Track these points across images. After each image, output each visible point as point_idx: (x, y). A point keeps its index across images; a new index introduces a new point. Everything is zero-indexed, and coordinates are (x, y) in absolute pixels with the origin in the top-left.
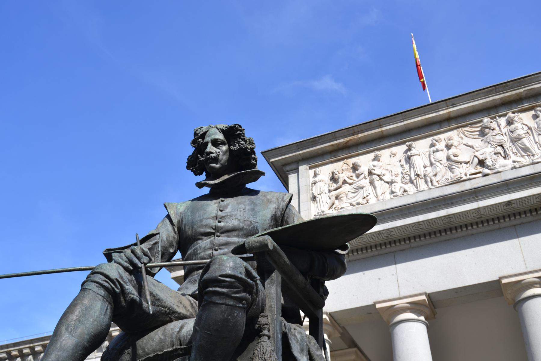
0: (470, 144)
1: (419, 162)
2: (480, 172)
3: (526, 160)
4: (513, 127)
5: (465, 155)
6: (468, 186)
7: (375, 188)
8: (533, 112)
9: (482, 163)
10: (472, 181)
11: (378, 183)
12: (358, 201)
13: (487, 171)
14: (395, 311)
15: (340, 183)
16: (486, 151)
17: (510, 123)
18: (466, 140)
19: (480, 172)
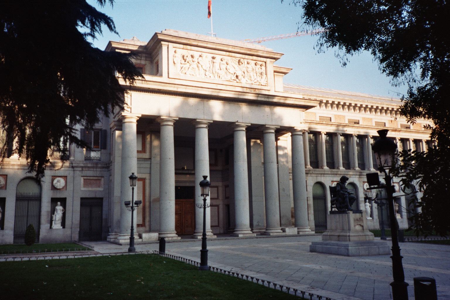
0: (235, 66)
1: (217, 65)
2: (235, 80)
3: (249, 82)
4: (248, 66)
5: (232, 70)
6: (231, 84)
7: (199, 69)
8: (255, 62)
9: (237, 76)
10: (233, 83)
11: (200, 68)
12: (192, 74)
13: (238, 81)
14: (200, 123)
15: (186, 62)
16: (239, 73)
17: (248, 63)
18: (233, 64)
19: (235, 80)
